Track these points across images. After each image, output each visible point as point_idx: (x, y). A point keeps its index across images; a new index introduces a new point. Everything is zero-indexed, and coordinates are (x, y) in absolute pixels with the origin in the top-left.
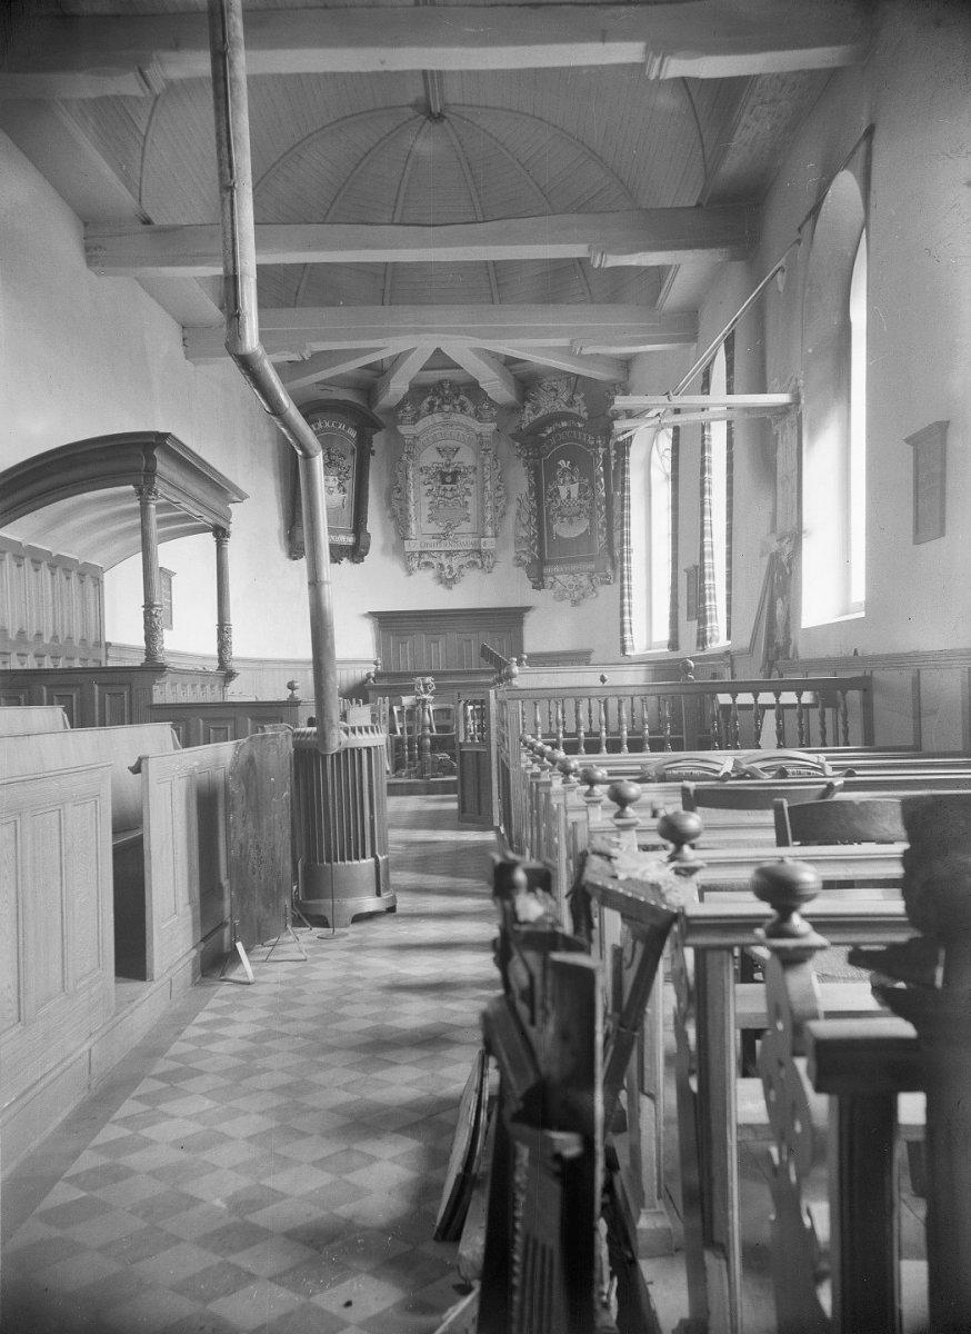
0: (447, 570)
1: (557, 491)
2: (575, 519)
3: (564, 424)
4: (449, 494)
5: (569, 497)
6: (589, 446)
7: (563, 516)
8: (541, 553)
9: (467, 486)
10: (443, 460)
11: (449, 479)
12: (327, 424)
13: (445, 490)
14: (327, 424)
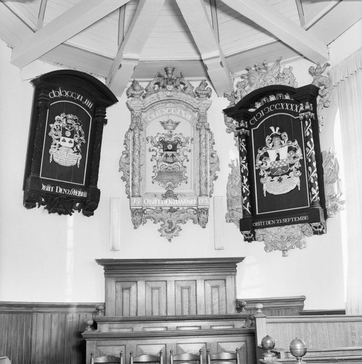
0: (167, 225)
1: (266, 155)
2: (285, 177)
3: (272, 98)
4: (170, 160)
5: (278, 159)
6: (297, 114)
7: (273, 177)
8: (252, 209)
10: (166, 132)
12: (67, 94)
13: (167, 156)
14: (67, 94)
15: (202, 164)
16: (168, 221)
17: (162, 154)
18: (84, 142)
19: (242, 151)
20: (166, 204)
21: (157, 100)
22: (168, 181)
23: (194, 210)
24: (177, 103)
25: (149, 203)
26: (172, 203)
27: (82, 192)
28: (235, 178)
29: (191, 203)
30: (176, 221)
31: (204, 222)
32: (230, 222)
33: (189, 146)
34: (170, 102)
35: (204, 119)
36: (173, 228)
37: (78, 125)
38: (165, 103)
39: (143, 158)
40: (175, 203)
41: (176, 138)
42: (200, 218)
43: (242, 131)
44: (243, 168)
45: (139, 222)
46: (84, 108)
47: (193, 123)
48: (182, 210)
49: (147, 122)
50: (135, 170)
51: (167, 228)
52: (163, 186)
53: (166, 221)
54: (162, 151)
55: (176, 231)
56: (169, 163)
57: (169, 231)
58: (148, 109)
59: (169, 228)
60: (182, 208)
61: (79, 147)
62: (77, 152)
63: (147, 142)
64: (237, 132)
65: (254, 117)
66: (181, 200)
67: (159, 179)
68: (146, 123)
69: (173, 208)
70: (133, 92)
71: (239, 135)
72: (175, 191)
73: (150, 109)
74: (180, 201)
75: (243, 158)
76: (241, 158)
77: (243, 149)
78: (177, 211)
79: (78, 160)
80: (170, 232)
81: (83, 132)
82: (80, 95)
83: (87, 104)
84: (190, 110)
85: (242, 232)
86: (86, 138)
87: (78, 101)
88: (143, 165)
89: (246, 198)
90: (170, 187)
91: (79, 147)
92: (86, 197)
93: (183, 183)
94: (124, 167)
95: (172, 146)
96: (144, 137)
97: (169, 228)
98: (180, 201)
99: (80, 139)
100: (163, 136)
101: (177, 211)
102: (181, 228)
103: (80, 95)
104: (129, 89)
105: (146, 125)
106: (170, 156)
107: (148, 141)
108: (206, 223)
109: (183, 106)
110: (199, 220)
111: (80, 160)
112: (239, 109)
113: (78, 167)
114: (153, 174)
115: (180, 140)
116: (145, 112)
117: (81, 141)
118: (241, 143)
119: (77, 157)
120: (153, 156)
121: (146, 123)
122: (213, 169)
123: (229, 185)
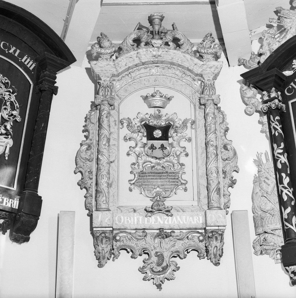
0: (154, 259)
4: (158, 153)
9: (183, 143)
10: (152, 111)
11: (158, 133)
13: (152, 147)
15: (210, 158)
16: (157, 253)
17: (145, 144)
18: (18, 119)
19: (277, 134)
20: (153, 223)
21: (137, 61)
22: (155, 187)
23: (199, 235)
24: (168, 68)
25: (124, 221)
26: (162, 222)
27: (11, 200)
28: (266, 181)
29: (194, 221)
30: (170, 253)
31: (218, 255)
32: (261, 253)
33: (189, 132)
34: (158, 67)
35: (211, 89)
36: (164, 264)
37: (10, 92)
38: (149, 69)
39: (114, 151)
40: (168, 221)
41: (168, 120)
42: (210, 248)
43: (275, 103)
44: (281, 161)
45: (107, 255)
46: (21, 67)
47: (194, 98)
48: (179, 234)
49: (121, 96)
50: (102, 168)
51: (154, 265)
52: (148, 195)
53: (153, 253)
54: (145, 140)
55: (169, 271)
56: (156, 158)
57: (159, 270)
58: (123, 77)
59: (158, 266)
60: (179, 231)
61: (9, 127)
62: (6, 134)
63: (121, 126)
64: (266, 106)
65: (292, 84)
66: (178, 217)
67: (140, 184)
68: (120, 98)
69: (165, 231)
70: (99, 50)
71: (269, 113)
72: (168, 203)
73: (127, 77)
74: (177, 219)
75: (279, 146)
76: (275, 146)
77: (278, 132)
78: (171, 236)
79: (6, 147)
80: (159, 271)
81: (18, 105)
82: (14, 48)
83: (26, 63)
84: (188, 78)
85: (287, 268)
86: (23, 114)
87: (10, 56)
88: (114, 161)
89: (289, 210)
90: (158, 197)
91: (9, 127)
92: (17, 208)
93: (180, 192)
94: (84, 165)
95: (160, 132)
96: (117, 119)
97: (159, 265)
98: (177, 219)
99: (12, 115)
100: (147, 116)
101: (171, 236)
102: (178, 266)
103: (14, 48)
104: (94, 46)
105: (120, 101)
106: (157, 147)
107: (122, 124)
108: (221, 256)
109: (178, 72)
110: (207, 251)
111: (11, 148)
112: (267, 70)
113: (7, 158)
114: (132, 177)
115: (174, 124)
116: (118, 80)
117: (13, 118)
118: (273, 122)
119: (5, 143)
120: (132, 148)
121: (120, 98)
122: (228, 169)
123: (255, 192)
